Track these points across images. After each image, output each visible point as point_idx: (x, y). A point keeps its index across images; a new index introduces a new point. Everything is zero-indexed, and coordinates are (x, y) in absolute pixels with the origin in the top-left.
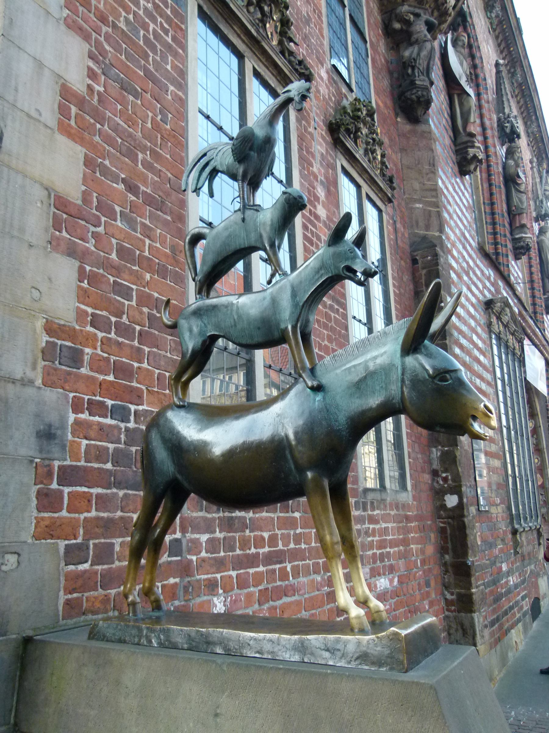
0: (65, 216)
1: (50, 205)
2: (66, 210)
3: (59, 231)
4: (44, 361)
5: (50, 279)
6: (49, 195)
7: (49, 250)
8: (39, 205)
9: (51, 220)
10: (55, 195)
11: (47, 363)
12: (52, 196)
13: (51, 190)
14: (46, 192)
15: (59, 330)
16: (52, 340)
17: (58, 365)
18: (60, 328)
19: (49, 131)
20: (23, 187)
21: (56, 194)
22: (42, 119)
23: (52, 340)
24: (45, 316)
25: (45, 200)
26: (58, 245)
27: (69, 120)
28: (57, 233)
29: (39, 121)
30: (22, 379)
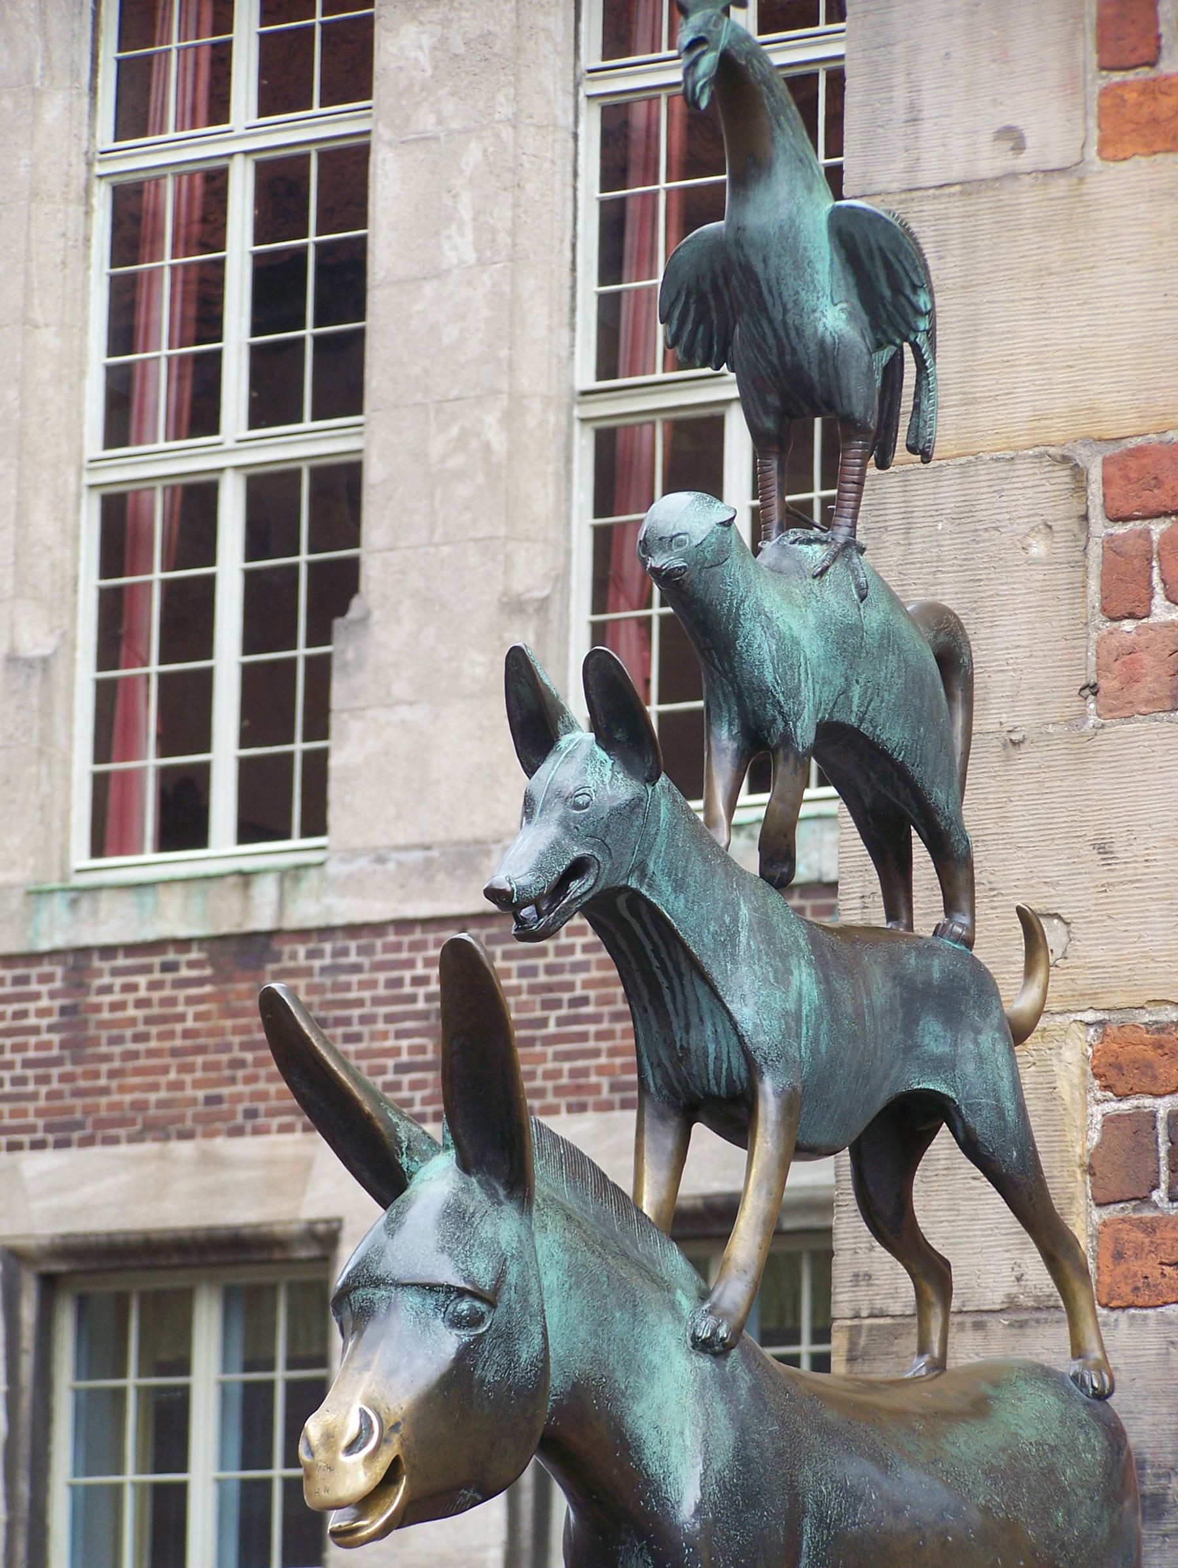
0: (1158, 528)
1: (1085, 518)
2: (1158, 498)
3: (1132, 616)
4: (1099, 1205)
5: (1103, 849)
6: (1079, 475)
7: (1093, 720)
8: (1039, 548)
9: (1094, 585)
10: (1106, 462)
11: (1113, 1211)
12: (1096, 474)
13: (1082, 455)
14: (1062, 475)
15: (1150, 1054)
16: (1125, 1106)
17: (1165, 1205)
18: (1159, 1045)
19: (1060, 186)
20: (964, 516)
21: (1111, 450)
22: (1025, 161)
23: (1125, 1106)
24: (1090, 1016)
25: (1061, 511)
26: (1132, 679)
27: (1152, 64)
28: (1128, 625)
29: (1014, 175)
30: (1012, 1306)
